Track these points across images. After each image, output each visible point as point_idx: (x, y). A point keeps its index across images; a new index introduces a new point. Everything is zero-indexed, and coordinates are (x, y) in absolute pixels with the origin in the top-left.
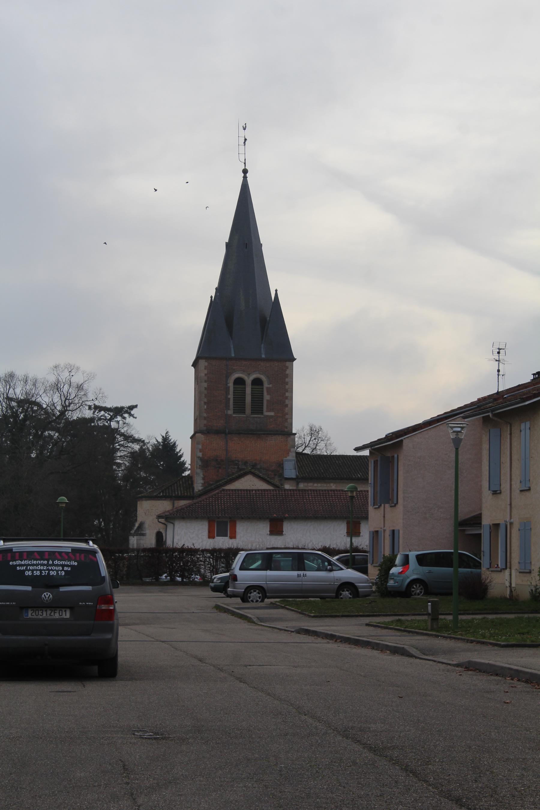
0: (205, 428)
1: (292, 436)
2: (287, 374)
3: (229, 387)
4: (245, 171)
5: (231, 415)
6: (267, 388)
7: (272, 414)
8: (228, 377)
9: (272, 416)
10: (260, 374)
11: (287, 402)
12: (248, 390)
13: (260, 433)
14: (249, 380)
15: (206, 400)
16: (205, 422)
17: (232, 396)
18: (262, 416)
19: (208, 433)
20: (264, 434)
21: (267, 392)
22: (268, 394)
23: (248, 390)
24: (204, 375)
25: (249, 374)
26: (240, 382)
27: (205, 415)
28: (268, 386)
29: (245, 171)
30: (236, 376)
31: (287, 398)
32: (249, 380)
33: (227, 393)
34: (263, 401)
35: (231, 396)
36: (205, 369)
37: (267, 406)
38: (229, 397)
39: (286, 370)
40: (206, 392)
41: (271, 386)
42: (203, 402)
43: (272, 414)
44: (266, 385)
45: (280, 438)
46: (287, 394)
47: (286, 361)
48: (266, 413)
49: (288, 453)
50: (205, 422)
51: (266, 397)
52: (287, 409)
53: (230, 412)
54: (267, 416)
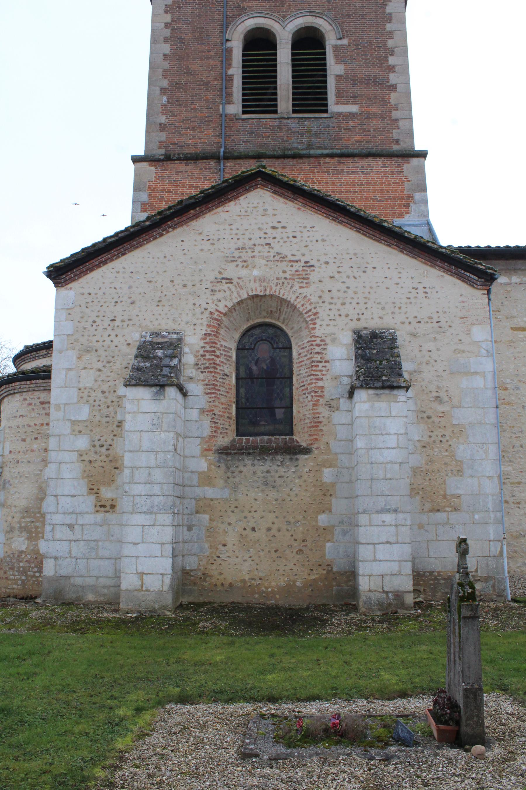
0: (163, 151)
1: (415, 161)
3: (229, 51)
5: (235, 115)
6: (336, 48)
7: (354, 108)
9: (353, 115)
11: (393, 78)
12: (284, 55)
13: (319, 152)
14: (284, 35)
15: (165, 83)
16: (163, 137)
18: (325, 115)
19: (168, 158)
20: (332, 156)
21: (336, 56)
22: (339, 59)
23: (284, 55)
27: (163, 119)
32: (284, 35)
33: (227, 62)
34: (325, 76)
35: (236, 70)
37: (338, 89)
38: (230, 72)
40: (166, 65)
42: (158, 89)
43: (354, 108)
48: (333, 107)
49: (408, 206)
50: (163, 137)
51: (334, 69)
52: (393, 95)
53: (235, 108)
54: (339, 114)
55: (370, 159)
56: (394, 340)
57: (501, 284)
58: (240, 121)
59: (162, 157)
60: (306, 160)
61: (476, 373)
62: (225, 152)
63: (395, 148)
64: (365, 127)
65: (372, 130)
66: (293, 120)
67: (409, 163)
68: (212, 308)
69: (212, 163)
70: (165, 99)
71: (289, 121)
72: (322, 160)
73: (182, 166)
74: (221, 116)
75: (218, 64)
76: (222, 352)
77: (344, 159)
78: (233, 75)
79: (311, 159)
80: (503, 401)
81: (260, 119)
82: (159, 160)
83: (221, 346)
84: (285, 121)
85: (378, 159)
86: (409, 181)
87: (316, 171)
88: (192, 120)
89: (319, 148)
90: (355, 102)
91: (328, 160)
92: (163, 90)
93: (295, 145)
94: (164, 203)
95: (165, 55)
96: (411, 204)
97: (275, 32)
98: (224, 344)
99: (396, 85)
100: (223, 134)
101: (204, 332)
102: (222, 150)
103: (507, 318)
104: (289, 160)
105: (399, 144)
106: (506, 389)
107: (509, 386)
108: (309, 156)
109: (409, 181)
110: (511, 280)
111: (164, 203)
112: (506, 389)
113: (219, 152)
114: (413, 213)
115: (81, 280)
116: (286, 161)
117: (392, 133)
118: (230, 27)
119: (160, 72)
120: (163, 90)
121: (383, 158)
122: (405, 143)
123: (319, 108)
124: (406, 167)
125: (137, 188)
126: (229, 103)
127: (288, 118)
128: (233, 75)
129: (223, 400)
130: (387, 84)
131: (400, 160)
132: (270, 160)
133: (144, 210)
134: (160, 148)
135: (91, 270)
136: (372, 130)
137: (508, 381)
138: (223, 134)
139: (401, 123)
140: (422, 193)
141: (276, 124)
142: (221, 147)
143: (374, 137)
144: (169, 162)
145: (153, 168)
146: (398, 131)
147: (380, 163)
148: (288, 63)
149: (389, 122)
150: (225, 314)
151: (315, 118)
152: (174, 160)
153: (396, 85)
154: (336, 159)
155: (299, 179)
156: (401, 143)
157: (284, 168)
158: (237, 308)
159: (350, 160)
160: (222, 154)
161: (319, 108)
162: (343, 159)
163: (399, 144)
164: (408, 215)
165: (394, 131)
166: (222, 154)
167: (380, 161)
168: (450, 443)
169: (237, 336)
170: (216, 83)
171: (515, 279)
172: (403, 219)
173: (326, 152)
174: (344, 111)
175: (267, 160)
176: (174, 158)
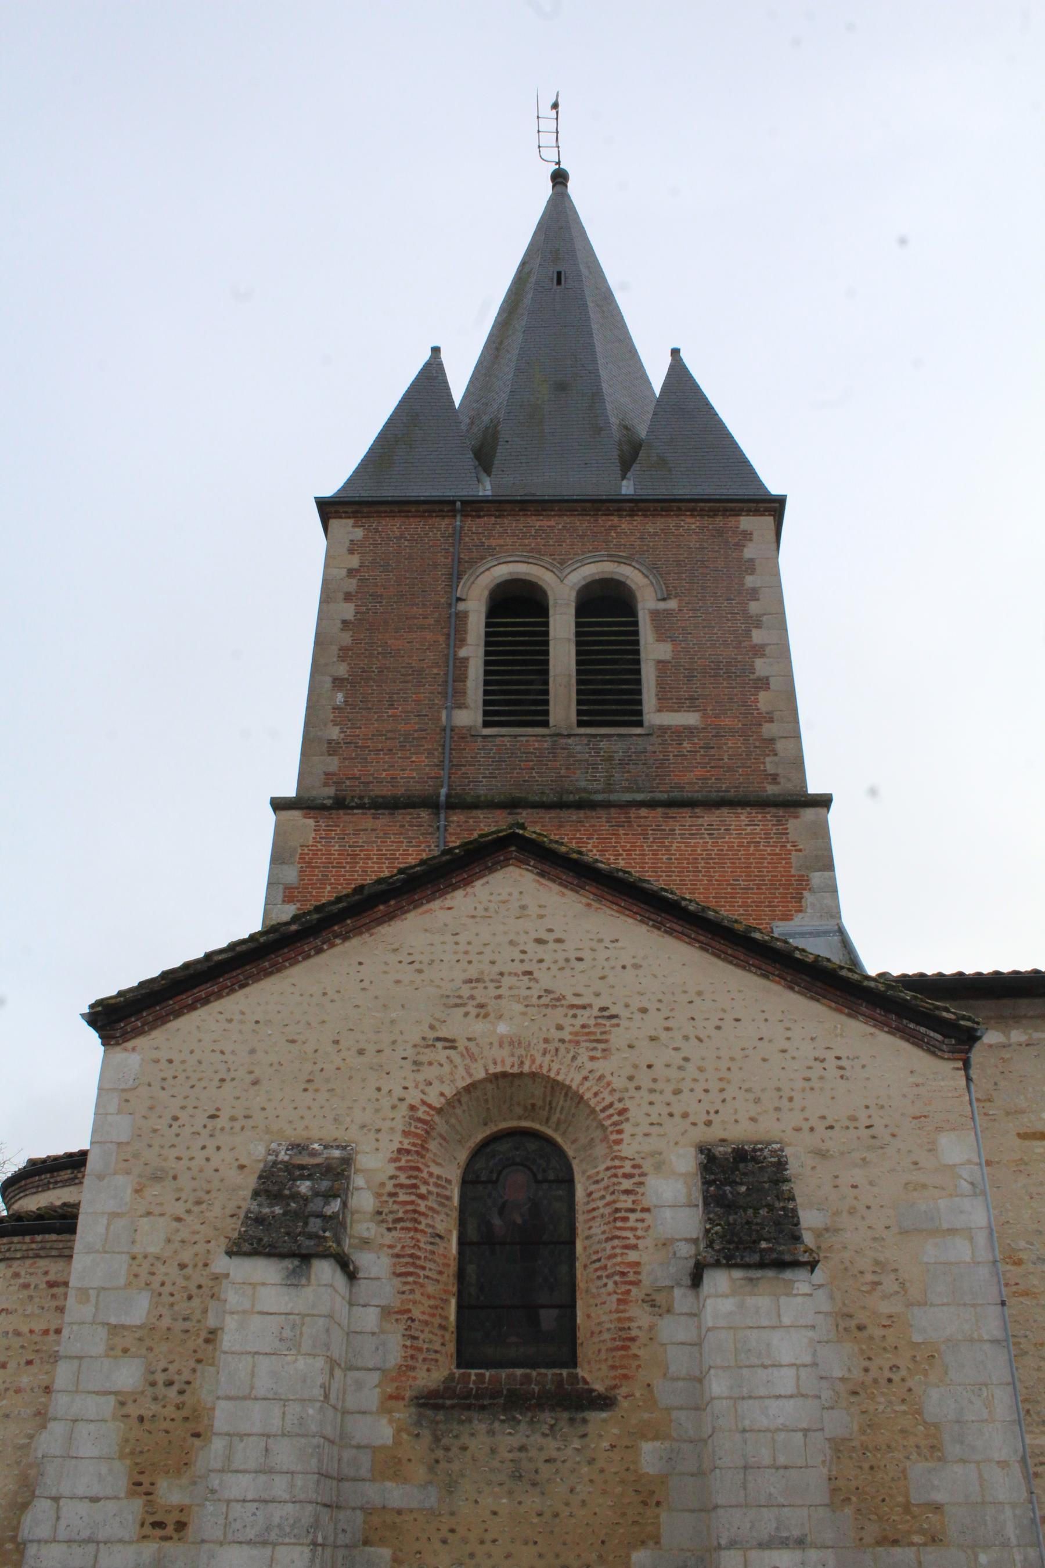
0: (331, 791)
2: (752, 560)
3: (462, 617)
4: (560, 178)
5: (470, 728)
6: (655, 614)
7: (690, 719)
8: (456, 574)
10: (612, 558)
11: (761, 667)
12: (562, 627)
13: (628, 797)
15: (342, 670)
16: (333, 764)
17: (481, 650)
18: (638, 731)
19: (340, 804)
20: (652, 804)
23: (562, 627)
24: (344, 572)
25: (562, 562)
26: (518, 607)
27: (334, 733)
28: (662, 605)
29: (560, 178)
31: (759, 651)
34: (638, 662)
35: (473, 651)
36: (351, 551)
37: (661, 685)
38: (463, 653)
39: (739, 546)
41: (672, 604)
42: (329, 679)
43: (690, 719)
44: (647, 602)
45: (741, 823)
46: (758, 636)
47: (737, 513)
48: (653, 716)
49: (800, 898)
50: (333, 764)
51: (653, 650)
52: (763, 696)
53: (469, 716)
54: (664, 729)
55: (725, 811)
56: (781, 1165)
57: (990, 1046)
58: (480, 739)
59: (329, 802)
60: (603, 813)
61: (952, 1231)
62: (448, 796)
63: (771, 789)
64: (712, 752)
65: (726, 757)
66: (577, 739)
67: (797, 817)
68: (414, 1097)
69: (423, 814)
70: (340, 697)
71: (570, 741)
72: (633, 813)
73: (367, 821)
74: (444, 730)
75: (442, 639)
76: (432, 1188)
77: (676, 810)
78: (467, 659)
79: (613, 810)
80: (1014, 1289)
81: (516, 736)
82: (323, 808)
83: (431, 1174)
84: (564, 741)
85: (739, 811)
86: (800, 850)
87: (622, 832)
88: (389, 735)
89: (628, 789)
90: (693, 708)
91: (643, 812)
92: (338, 682)
93: (583, 784)
94: (329, 888)
95: (344, 622)
96: (806, 893)
97: (545, 586)
98: (436, 1170)
99: (767, 678)
100: (447, 762)
101: (396, 1145)
102: (443, 791)
103: (1008, 1114)
104: (570, 811)
105: (779, 783)
106: (1019, 1263)
107: (1024, 1256)
108: (607, 805)
109: (800, 850)
110: (1008, 1037)
111: (329, 888)
112: (1019, 1263)
113: (438, 796)
114: (809, 910)
115: (155, 1033)
116: (564, 814)
117: (764, 763)
118: (466, 577)
119: (334, 650)
120: (338, 682)
121: (748, 809)
122: (789, 780)
123: (626, 718)
124: (792, 824)
125: (278, 858)
126: (460, 708)
127: (569, 736)
128: (467, 659)
129: (431, 1289)
130: (752, 677)
131: (781, 812)
132: (534, 810)
133: (288, 899)
134: (326, 784)
135: (178, 1014)
136: (726, 757)
137: (1022, 1244)
138: (447, 762)
139: (780, 746)
140: (826, 874)
141: (546, 745)
142: (442, 786)
143: (730, 769)
144: (341, 812)
145: (311, 822)
146: (776, 759)
147: (743, 818)
148: (569, 640)
149: (757, 744)
150: (440, 1111)
151: (619, 735)
152: (353, 808)
153: (767, 678)
154: (660, 810)
155: (590, 847)
156: (782, 780)
157: (560, 826)
158: (465, 1099)
159: (686, 812)
160: (443, 798)
161: (626, 718)
162: (672, 812)
163: (779, 783)
164: (800, 915)
165: (768, 759)
166: (443, 798)
167: (744, 815)
168: (910, 1383)
169: (463, 1156)
170: (435, 671)
171: (1017, 1036)
172: (791, 923)
173: (639, 797)
174: (674, 723)
175: (529, 811)
176: (353, 804)
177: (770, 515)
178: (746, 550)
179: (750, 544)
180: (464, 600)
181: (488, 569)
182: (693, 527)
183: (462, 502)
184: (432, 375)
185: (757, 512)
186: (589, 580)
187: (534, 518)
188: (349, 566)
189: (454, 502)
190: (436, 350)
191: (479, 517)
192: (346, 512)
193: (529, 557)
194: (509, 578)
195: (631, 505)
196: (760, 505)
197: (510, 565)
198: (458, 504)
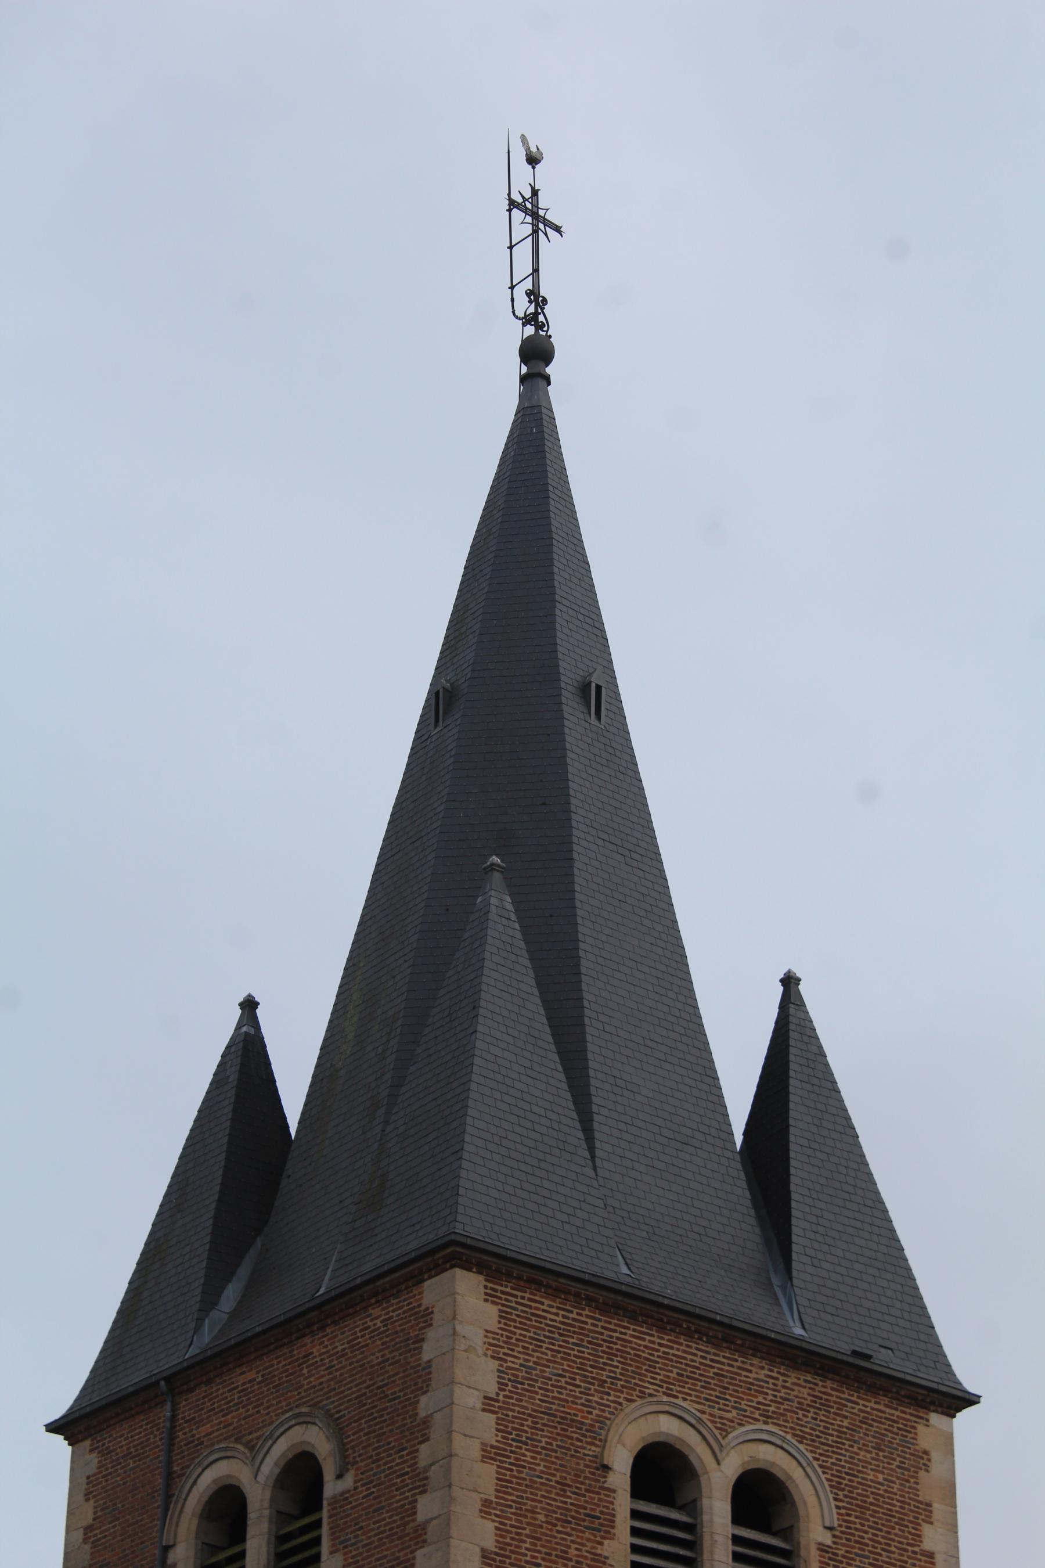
4: (536, 354)
6: (334, 1501)
29: (536, 354)
30: (207, 1480)
47: (418, 1279)
177: (452, 1267)
178: (426, 1346)
179: (430, 1334)
180: (173, 1546)
181: (195, 1483)
182: (378, 1322)
183: (168, 1379)
184: (247, 1059)
185: (438, 1269)
186: (282, 1463)
187: (238, 1371)
188: (84, 1524)
189: (157, 1383)
190: (249, 1005)
191: (191, 1390)
192: (80, 1432)
193: (225, 1449)
194: (215, 1487)
195: (315, 1313)
196: (436, 1256)
197: (214, 1466)
198: (162, 1383)
